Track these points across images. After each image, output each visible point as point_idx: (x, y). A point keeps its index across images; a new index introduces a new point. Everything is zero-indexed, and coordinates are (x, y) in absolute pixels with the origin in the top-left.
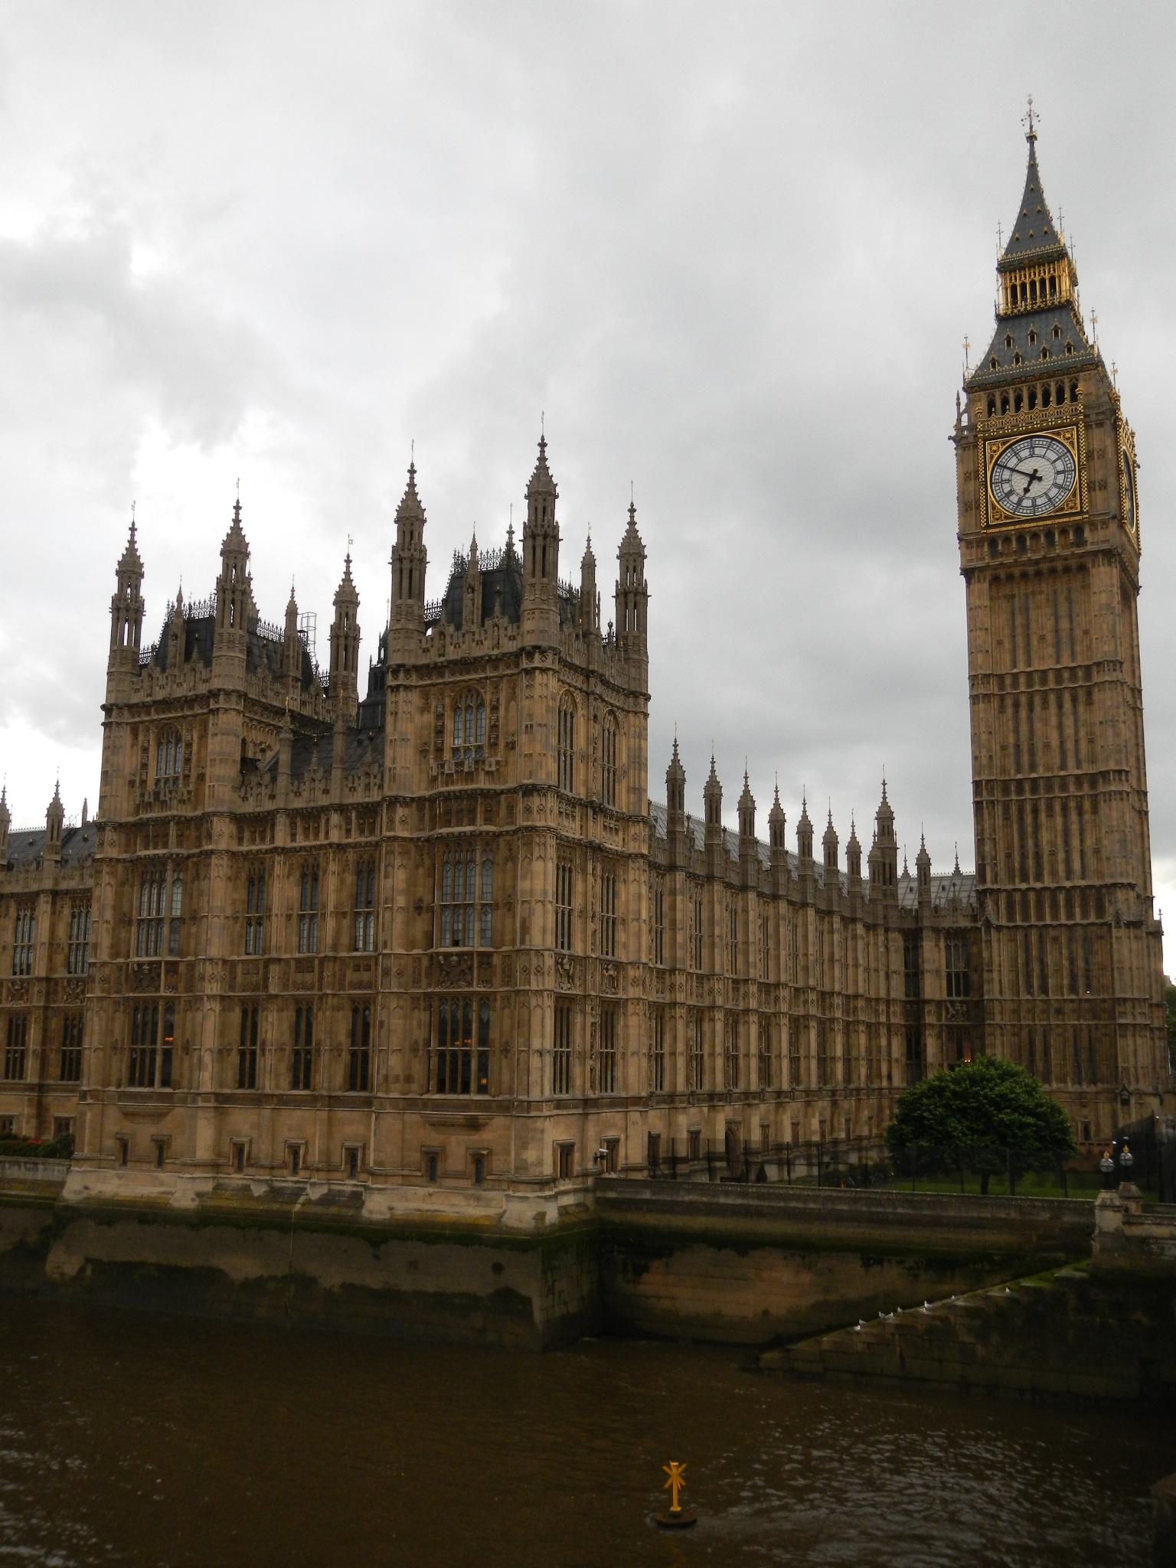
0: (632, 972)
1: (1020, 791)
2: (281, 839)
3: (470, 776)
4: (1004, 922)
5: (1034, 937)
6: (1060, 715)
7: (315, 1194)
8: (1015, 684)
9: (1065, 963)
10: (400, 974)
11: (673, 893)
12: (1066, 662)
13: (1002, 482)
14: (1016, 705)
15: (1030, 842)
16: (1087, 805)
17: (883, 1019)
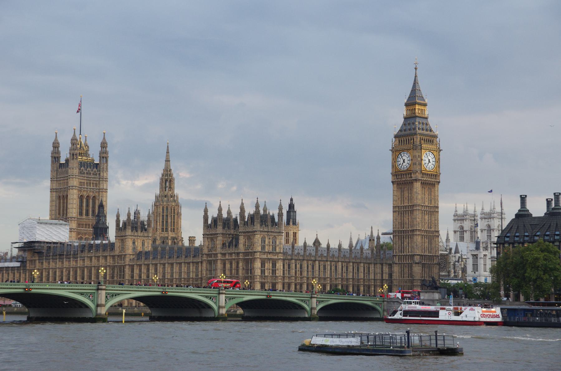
0: (279, 278)
1: (401, 233)
2: (227, 257)
3: (248, 250)
4: (398, 262)
5: (402, 266)
6: (408, 216)
7: (232, 311)
8: (401, 209)
9: (407, 271)
10: (241, 279)
11: (292, 264)
12: (410, 204)
13: (399, 161)
14: (401, 213)
15: (402, 245)
16: (412, 236)
17: (373, 284)
